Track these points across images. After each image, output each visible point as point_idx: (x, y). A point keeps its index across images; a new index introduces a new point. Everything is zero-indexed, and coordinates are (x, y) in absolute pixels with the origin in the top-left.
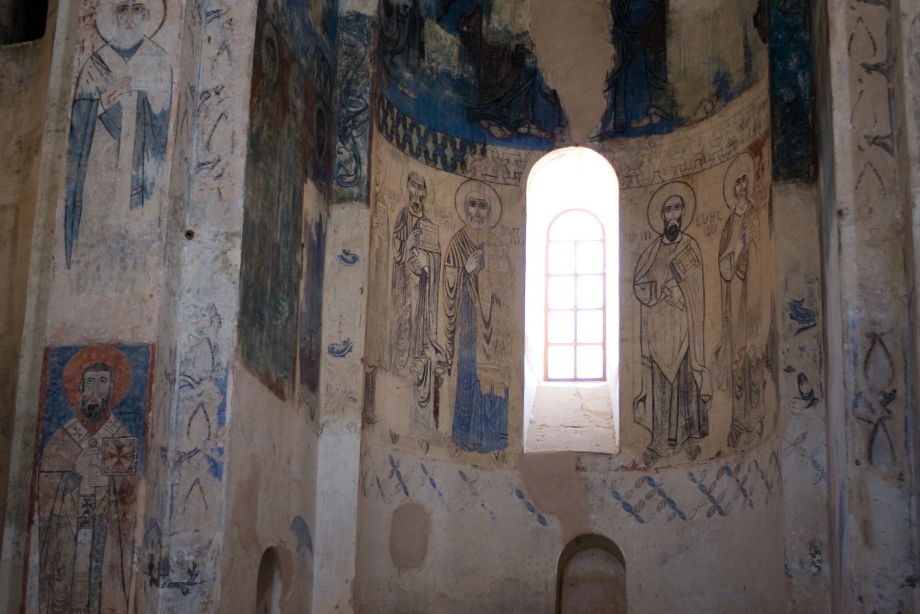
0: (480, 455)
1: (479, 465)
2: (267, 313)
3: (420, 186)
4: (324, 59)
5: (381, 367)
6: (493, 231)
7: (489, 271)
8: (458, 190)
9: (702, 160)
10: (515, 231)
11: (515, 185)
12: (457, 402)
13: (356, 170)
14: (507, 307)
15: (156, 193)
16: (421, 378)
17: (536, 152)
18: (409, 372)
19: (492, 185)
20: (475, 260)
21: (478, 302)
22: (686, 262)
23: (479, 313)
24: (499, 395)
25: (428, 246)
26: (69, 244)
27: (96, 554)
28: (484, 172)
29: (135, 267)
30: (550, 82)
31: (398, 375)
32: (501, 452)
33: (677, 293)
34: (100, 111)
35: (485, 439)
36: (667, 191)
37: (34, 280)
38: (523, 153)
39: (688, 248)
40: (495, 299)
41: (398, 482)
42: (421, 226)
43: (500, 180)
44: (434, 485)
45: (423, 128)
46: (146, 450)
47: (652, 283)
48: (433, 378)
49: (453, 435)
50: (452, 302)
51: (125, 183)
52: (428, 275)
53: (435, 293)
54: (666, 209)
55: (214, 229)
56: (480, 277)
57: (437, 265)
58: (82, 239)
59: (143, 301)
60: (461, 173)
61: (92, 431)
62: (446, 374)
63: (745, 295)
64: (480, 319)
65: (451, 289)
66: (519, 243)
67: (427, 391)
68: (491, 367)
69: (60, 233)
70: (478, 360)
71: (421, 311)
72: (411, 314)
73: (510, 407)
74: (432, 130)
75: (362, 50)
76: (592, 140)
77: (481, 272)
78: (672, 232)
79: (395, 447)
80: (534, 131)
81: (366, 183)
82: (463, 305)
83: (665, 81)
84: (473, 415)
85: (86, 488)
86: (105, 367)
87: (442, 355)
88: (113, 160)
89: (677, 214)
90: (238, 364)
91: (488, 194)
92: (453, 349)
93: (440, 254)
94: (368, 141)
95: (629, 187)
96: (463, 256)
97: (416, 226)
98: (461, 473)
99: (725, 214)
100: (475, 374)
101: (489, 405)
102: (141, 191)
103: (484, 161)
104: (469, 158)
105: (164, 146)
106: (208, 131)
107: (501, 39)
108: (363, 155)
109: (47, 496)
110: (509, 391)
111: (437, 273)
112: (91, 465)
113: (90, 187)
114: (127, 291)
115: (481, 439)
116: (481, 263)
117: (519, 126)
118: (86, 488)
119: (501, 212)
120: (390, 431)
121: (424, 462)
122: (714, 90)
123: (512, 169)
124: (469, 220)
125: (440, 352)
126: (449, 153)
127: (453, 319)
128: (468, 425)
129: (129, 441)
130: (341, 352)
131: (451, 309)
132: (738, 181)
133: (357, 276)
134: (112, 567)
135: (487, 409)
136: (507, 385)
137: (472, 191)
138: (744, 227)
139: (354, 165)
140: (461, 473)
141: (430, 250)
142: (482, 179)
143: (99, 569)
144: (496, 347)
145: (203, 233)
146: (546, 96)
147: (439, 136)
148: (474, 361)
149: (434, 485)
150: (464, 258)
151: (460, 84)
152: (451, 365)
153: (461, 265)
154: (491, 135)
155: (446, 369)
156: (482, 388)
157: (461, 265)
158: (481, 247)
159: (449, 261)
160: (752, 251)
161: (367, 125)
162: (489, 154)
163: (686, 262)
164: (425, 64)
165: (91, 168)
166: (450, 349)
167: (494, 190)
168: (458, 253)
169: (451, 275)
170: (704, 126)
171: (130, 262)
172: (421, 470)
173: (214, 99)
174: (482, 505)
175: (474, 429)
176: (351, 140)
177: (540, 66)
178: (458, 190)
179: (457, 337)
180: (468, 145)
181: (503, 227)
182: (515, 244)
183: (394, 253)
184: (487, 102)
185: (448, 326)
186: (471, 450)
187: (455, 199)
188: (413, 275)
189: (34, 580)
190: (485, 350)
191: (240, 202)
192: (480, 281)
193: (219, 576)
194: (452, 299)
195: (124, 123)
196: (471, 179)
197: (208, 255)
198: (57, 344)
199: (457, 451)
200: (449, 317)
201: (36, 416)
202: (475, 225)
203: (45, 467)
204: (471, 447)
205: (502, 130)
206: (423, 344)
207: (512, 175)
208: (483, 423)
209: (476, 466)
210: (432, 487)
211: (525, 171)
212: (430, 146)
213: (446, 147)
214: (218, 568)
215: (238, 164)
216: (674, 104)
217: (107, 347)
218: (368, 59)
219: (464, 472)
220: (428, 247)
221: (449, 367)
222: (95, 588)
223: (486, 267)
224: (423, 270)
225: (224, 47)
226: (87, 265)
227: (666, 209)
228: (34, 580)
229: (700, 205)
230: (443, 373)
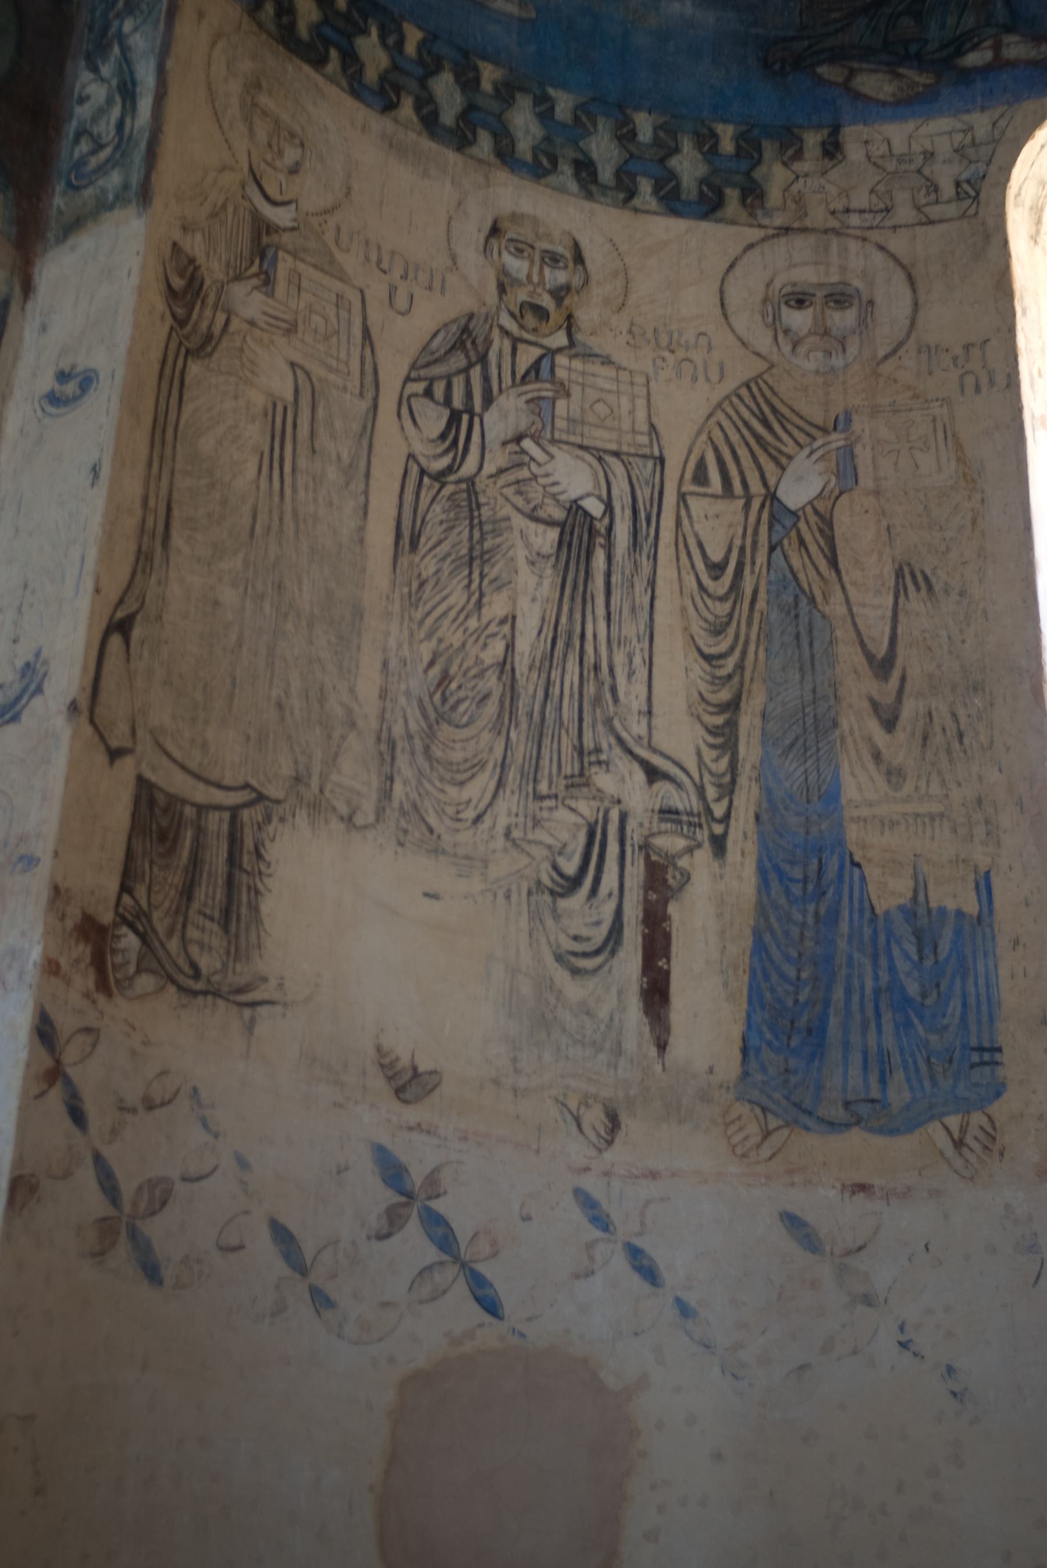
0: (881, 1141)
1: (877, 1182)
3: (553, 259)
5: (317, 808)
6: (887, 368)
7: (877, 493)
8: (732, 267)
10: (976, 352)
11: (963, 216)
12: (759, 947)
13: (120, 125)
14: (962, 594)
16: (570, 868)
18: (500, 842)
19: (875, 236)
20: (820, 467)
21: (839, 595)
23: (843, 633)
24: (951, 905)
25: (599, 433)
28: (839, 205)
31: (437, 851)
32: (977, 1118)
35: (899, 1076)
38: (981, 122)
41: (432, 1254)
42: (561, 374)
43: (904, 213)
44: (649, 1273)
48: (636, 872)
49: (746, 1074)
50: (722, 609)
52: (601, 526)
53: (640, 585)
56: (843, 521)
57: (643, 494)
60: (743, 216)
62: (704, 855)
64: (849, 655)
65: (717, 569)
66: (992, 383)
67: (608, 910)
68: (909, 808)
70: (850, 791)
72: (510, 647)
73: (1003, 942)
77: (844, 499)
79: (412, 1114)
80: (1016, 48)
81: (143, 145)
82: (774, 616)
84: (838, 993)
87: (679, 786)
92: (733, 767)
93: (661, 460)
94: (162, 26)
96: (763, 459)
98: (792, 1221)
100: (840, 843)
101: (912, 950)
103: (834, 174)
110: (996, 882)
115: (883, 1081)
117: (960, 53)
119: (916, 305)
120: (379, 1049)
121: (592, 1185)
123: (945, 175)
124: (787, 349)
125: (666, 777)
127: (730, 663)
128: (816, 1032)
131: (717, 630)
135: (902, 965)
136: (983, 861)
140: (792, 1221)
141: (613, 447)
142: (833, 223)
144: (925, 738)
148: (832, 797)
149: (649, 1273)
150: (769, 467)
152: (726, 818)
153: (756, 487)
154: (858, 96)
155: (702, 835)
156: (871, 888)
157: (756, 487)
158: (842, 423)
159: (701, 477)
162: (854, 152)
166: (724, 764)
167: (881, 248)
168: (742, 452)
172: (577, 1216)
174: (903, 1345)
175: (846, 1046)
176: (116, 50)
178: (732, 267)
179: (748, 721)
181: (927, 350)
182: (978, 389)
184: (835, 15)
185: (703, 687)
186: (833, 1126)
187: (722, 292)
188: (519, 521)
190: (877, 756)
192: (840, 531)
194: (722, 599)
199: (767, 1134)
200: (708, 658)
202: (810, 362)
204: (839, 1114)
205: (899, 76)
206: (580, 751)
207: (948, 190)
208: (887, 1017)
209: (862, 1188)
210: (636, 1283)
211: (993, 168)
213: (677, 150)
219: (809, 1218)
220: (602, 438)
221: (718, 829)
223: (866, 481)
224: (575, 508)
230: (690, 851)
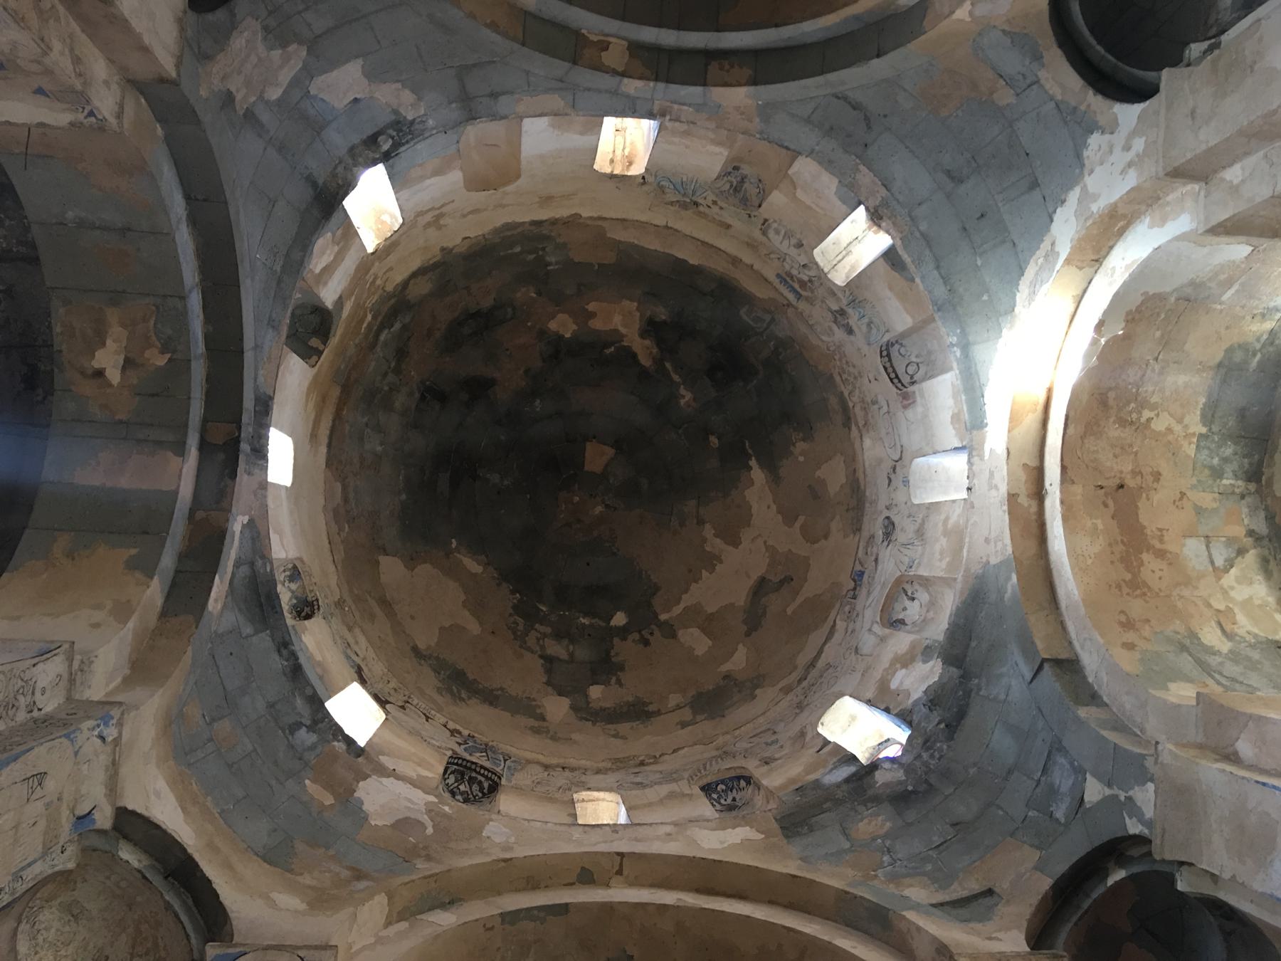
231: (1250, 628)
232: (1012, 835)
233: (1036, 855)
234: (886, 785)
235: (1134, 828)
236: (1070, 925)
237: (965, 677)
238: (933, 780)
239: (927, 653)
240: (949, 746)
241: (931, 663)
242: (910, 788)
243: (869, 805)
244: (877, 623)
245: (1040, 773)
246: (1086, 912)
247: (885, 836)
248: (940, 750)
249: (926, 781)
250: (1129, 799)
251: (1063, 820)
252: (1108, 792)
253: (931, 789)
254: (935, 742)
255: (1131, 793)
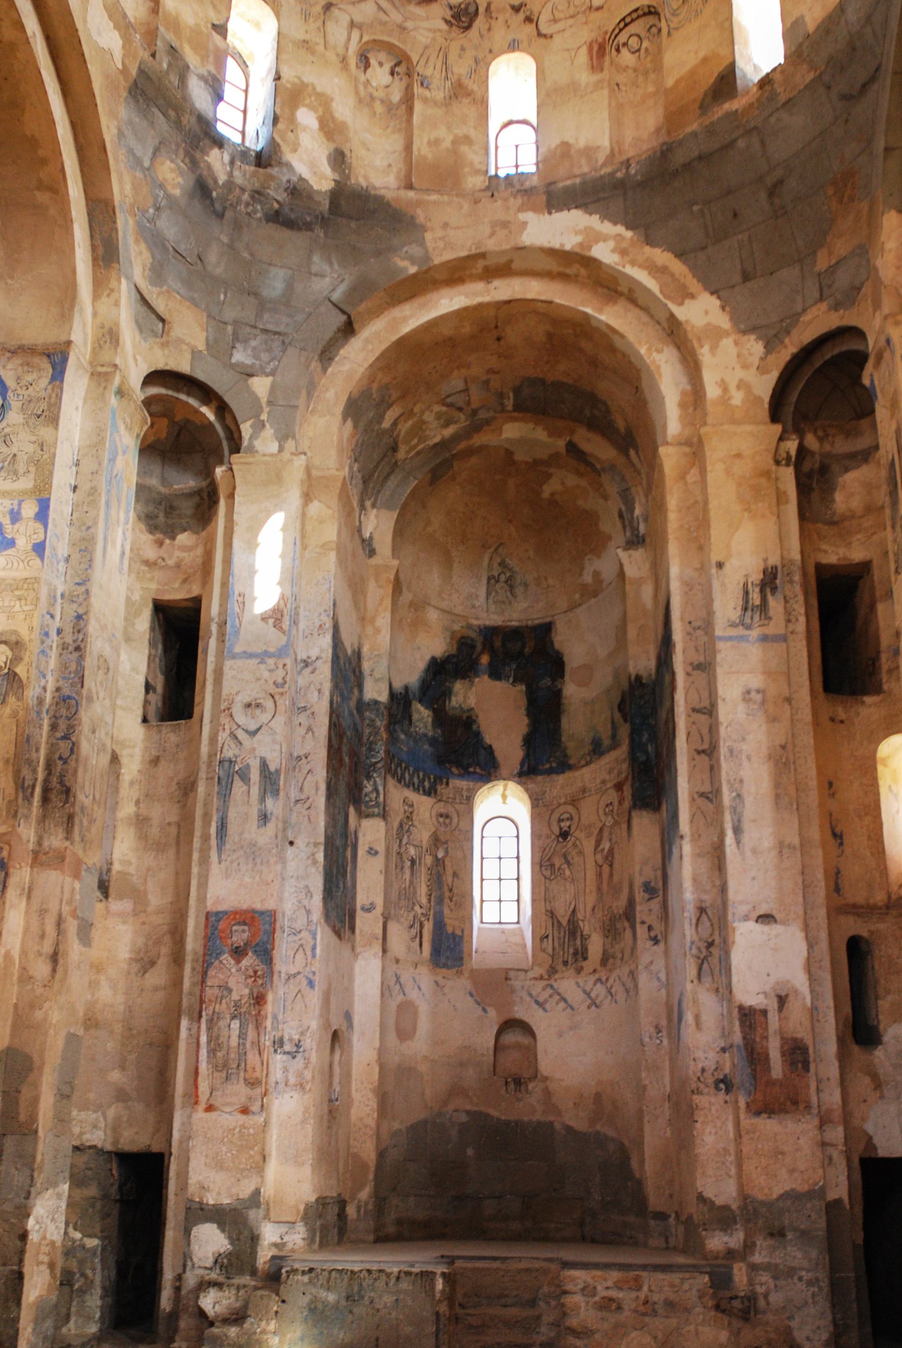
2: (334, 889)
4: (357, 730)
9: (584, 790)
15: (274, 820)
17: (479, 784)
22: (574, 853)
26: (220, 849)
27: (242, 1036)
29: (262, 863)
30: (488, 740)
33: (567, 872)
34: (237, 768)
36: (562, 809)
37: (195, 870)
38: (471, 784)
39: (575, 845)
40: (455, 875)
45: (411, 769)
46: (272, 973)
47: (552, 865)
51: (254, 812)
54: (560, 820)
55: (306, 840)
58: (227, 846)
59: (268, 884)
61: (238, 962)
63: (611, 875)
64: (446, 888)
69: (213, 842)
71: (411, 882)
74: (417, 770)
75: (378, 723)
76: (514, 776)
78: (564, 835)
80: (478, 770)
83: (560, 740)
85: (235, 996)
86: (245, 924)
88: (246, 798)
89: (568, 823)
90: (322, 921)
91: (450, 810)
95: (537, 806)
97: (408, 831)
99: (600, 825)
102: (264, 818)
104: (439, 788)
105: (278, 790)
106: (301, 780)
107: (457, 712)
108: (381, 789)
109: (210, 1001)
111: (420, 859)
112: (238, 983)
113: (232, 814)
114: (257, 878)
116: (447, 852)
118: (235, 996)
122: (591, 748)
123: (465, 794)
126: (427, 784)
129: (261, 968)
130: (368, 909)
132: (607, 806)
133: (378, 863)
134: (253, 1043)
137: (441, 808)
138: (611, 834)
139: (374, 795)
143: (244, 1044)
145: (300, 842)
146: (485, 749)
147: (421, 774)
151: (433, 742)
158: (446, 843)
160: (616, 849)
161: (382, 771)
162: (451, 785)
163: (574, 853)
164: (412, 729)
165: (232, 803)
169: (429, 860)
170: (585, 770)
171: (258, 861)
173: (304, 761)
177: (481, 729)
180: (438, 779)
183: (396, 847)
189: (203, 1052)
191: (322, 824)
193: (314, 1047)
195: (252, 776)
196: (440, 801)
197: (303, 855)
198: (214, 910)
201: (201, 953)
203: (209, 983)
212: (416, 780)
214: (314, 1043)
215: (321, 801)
216: (566, 756)
217: (246, 912)
218: (382, 729)
220: (415, 843)
222: (242, 1054)
225: (309, 729)
226: (232, 862)
227: (560, 820)
228: (203, 1052)
229: (582, 818)
231: (402, 434)
232: (209, 316)
233: (201, 346)
234: (209, 167)
235: (246, 429)
236: (163, 391)
237: (324, 221)
238: (229, 214)
239: (339, 159)
240: (260, 219)
241: (328, 171)
242: (214, 194)
243: (187, 160)
244: (361, 37)
245: (261, 326)
246: (177, 399)
247: (168, 196)
248: (255, 212)
249: (225, 209)
250: (264, 426)
251: (233, 361)
252: (264, 401)
253: (221, 216)
254: (260, 202)
255: (267, 425)
